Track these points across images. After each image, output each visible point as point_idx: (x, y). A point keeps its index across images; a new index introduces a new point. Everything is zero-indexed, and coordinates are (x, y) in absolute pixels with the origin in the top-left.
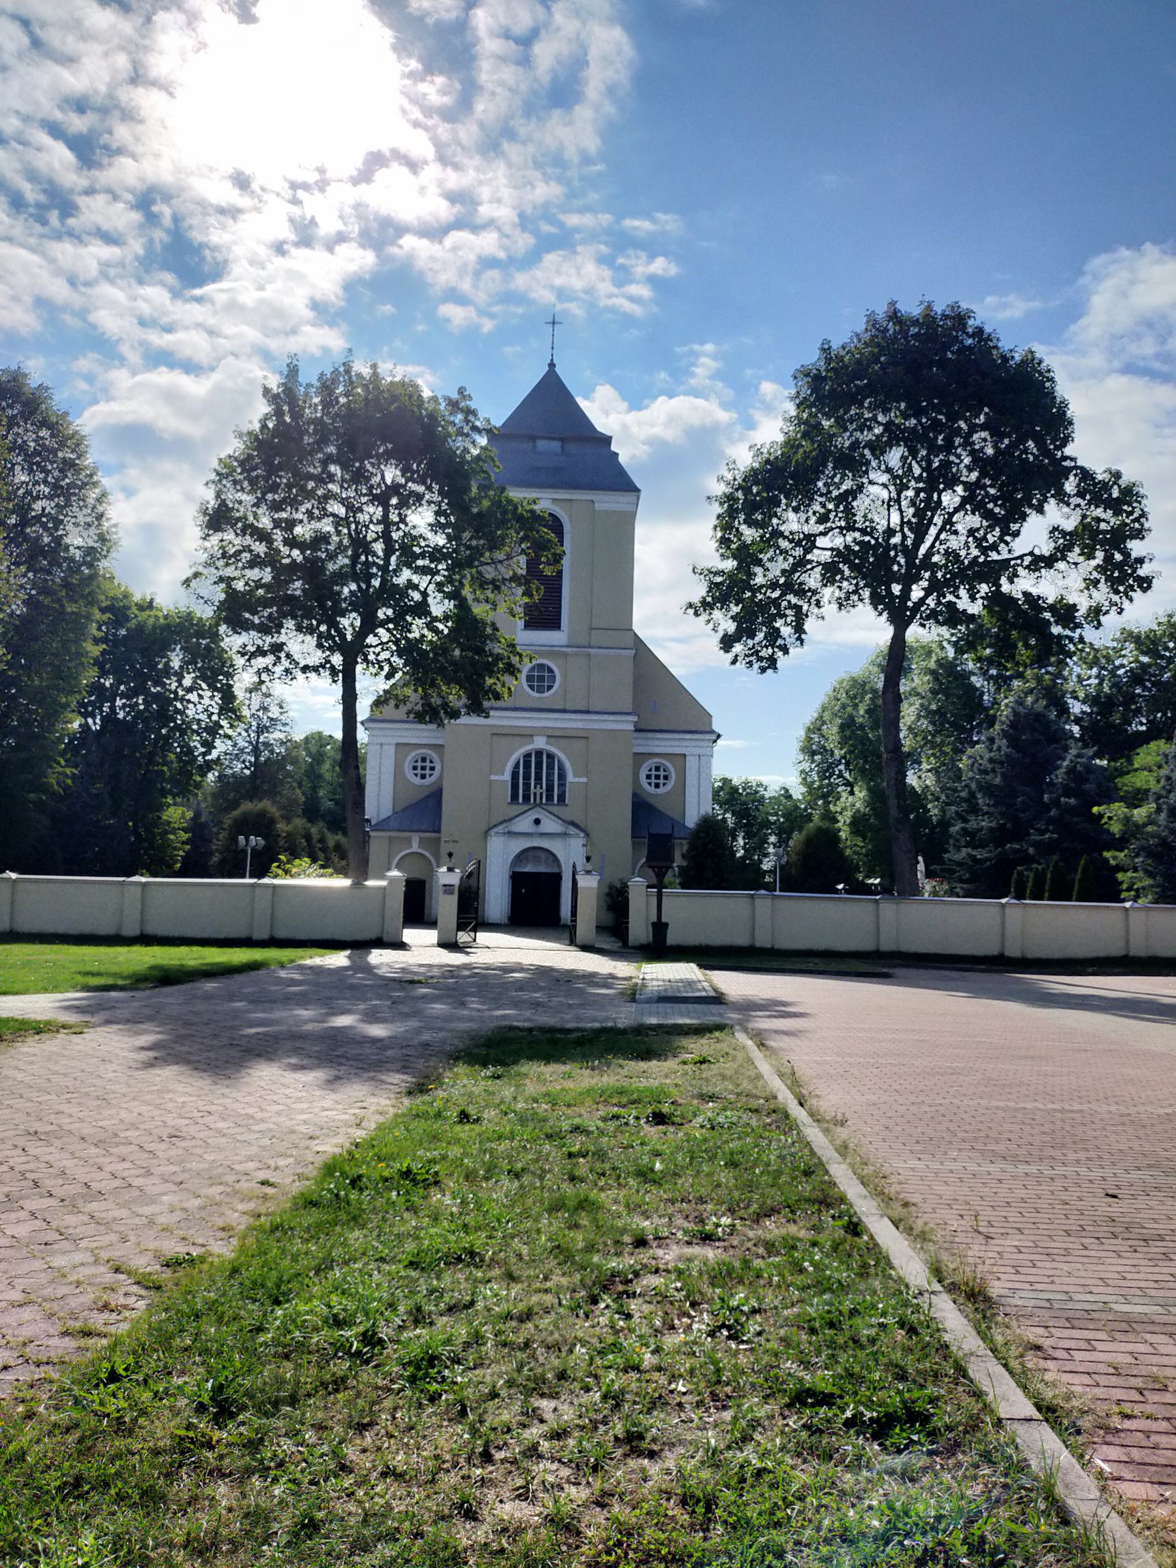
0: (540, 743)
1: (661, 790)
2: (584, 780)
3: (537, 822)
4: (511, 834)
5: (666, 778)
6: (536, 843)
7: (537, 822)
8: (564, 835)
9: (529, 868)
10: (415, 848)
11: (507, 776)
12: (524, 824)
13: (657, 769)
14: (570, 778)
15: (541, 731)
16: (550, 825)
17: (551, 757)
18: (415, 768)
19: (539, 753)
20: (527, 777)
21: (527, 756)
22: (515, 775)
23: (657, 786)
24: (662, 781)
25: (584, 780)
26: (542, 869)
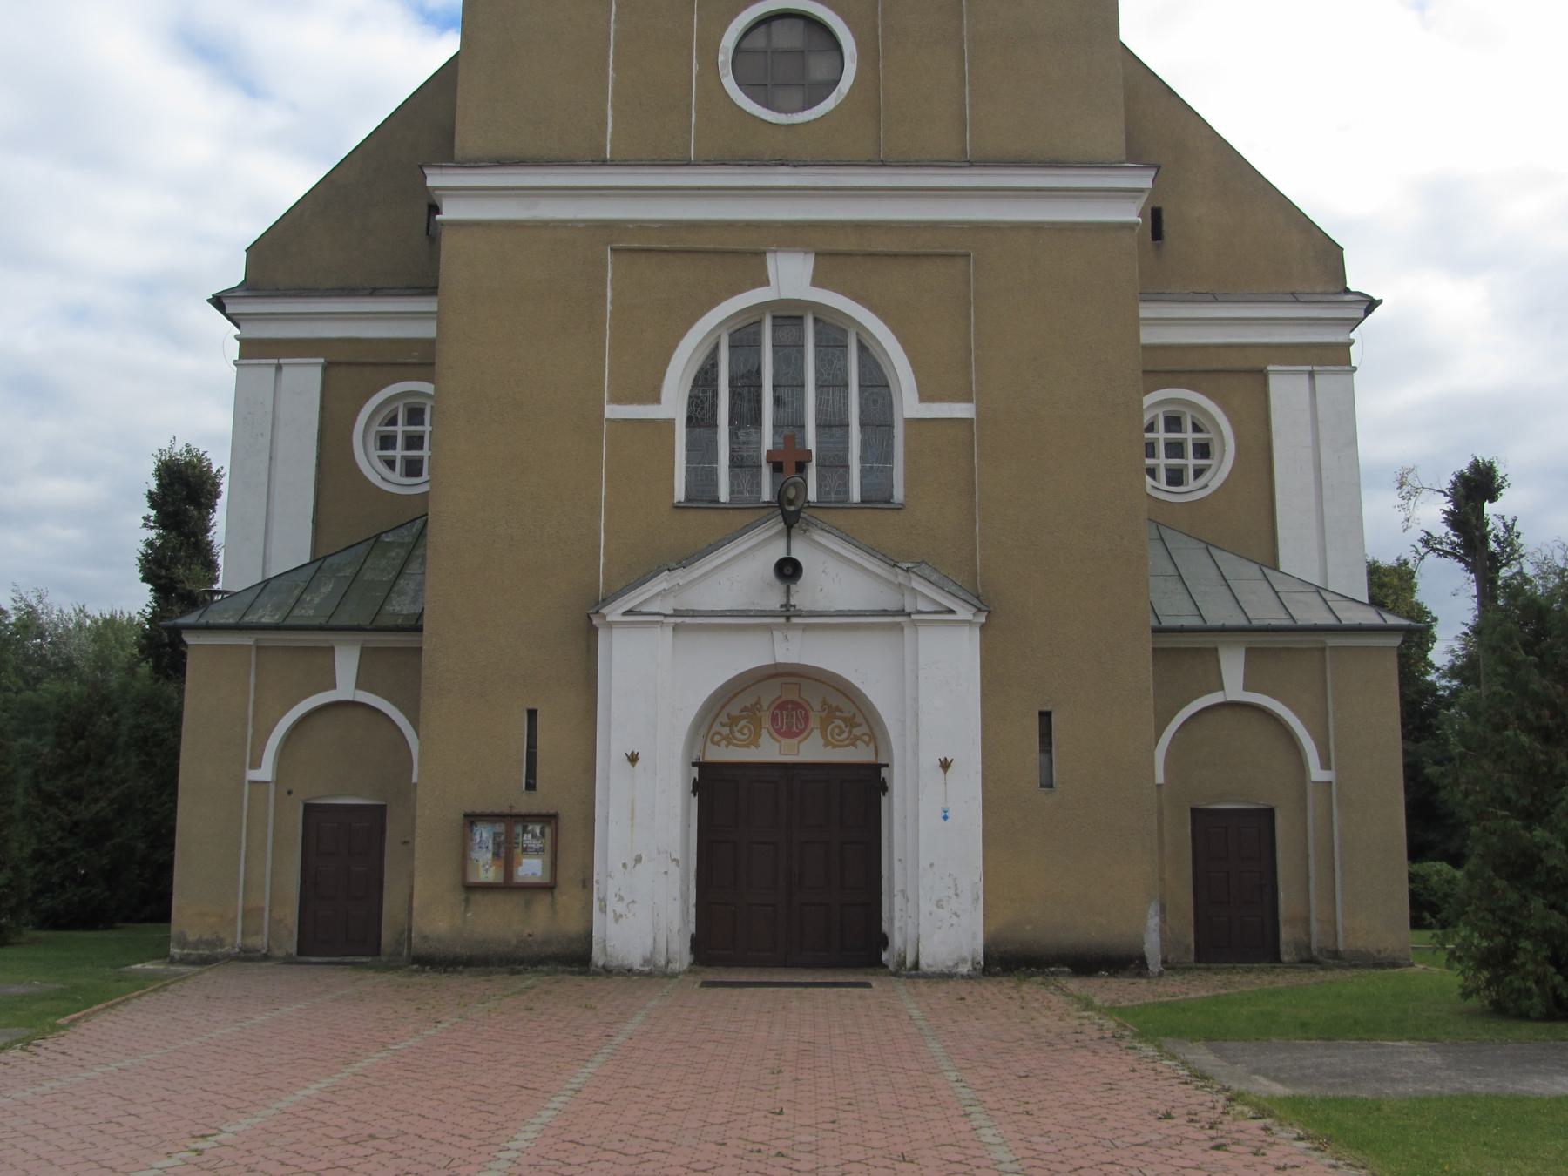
0: (791, 276)
1: (1193, 491)
2: (963, 411)
3: (788, 570)
4: (687, 622)
5: (1203, 450)
6: (793, 650)
7: (788, 570)
8: (894, 619)
9: (769, 750)
10: (345, 687)
11: (673, 404)
12: (738, 573)
13: (1173, 423)
14: (909, 404)
15: (792, 235)
16: (837, 576)
17: (833, 332)
18: (386, 442)
19: (788, 316)
20: (746, 416)
21: (744, 336)
22: (700, 414)
23: (1175, 477)
24: (1190, 462)
25: (963, 411)
26: (811, 750)
